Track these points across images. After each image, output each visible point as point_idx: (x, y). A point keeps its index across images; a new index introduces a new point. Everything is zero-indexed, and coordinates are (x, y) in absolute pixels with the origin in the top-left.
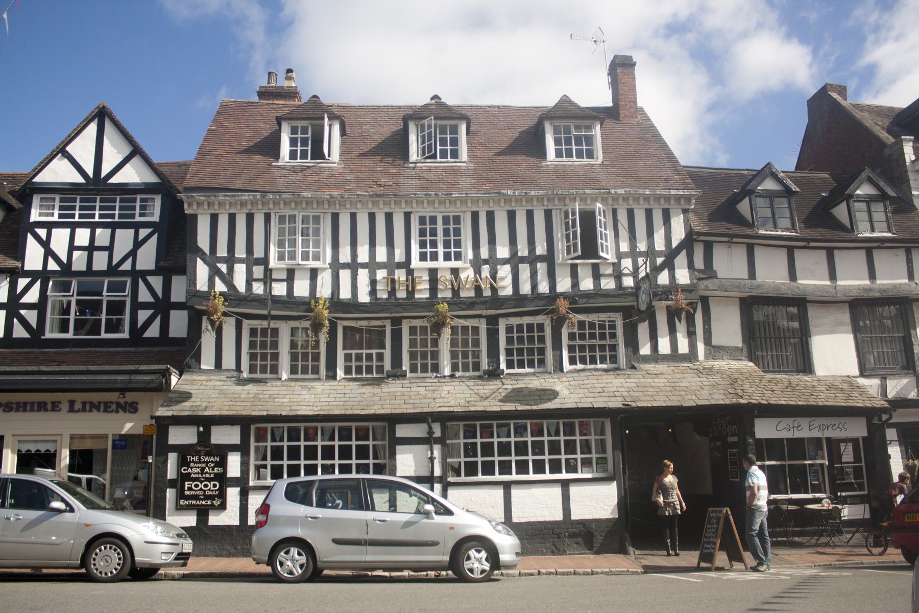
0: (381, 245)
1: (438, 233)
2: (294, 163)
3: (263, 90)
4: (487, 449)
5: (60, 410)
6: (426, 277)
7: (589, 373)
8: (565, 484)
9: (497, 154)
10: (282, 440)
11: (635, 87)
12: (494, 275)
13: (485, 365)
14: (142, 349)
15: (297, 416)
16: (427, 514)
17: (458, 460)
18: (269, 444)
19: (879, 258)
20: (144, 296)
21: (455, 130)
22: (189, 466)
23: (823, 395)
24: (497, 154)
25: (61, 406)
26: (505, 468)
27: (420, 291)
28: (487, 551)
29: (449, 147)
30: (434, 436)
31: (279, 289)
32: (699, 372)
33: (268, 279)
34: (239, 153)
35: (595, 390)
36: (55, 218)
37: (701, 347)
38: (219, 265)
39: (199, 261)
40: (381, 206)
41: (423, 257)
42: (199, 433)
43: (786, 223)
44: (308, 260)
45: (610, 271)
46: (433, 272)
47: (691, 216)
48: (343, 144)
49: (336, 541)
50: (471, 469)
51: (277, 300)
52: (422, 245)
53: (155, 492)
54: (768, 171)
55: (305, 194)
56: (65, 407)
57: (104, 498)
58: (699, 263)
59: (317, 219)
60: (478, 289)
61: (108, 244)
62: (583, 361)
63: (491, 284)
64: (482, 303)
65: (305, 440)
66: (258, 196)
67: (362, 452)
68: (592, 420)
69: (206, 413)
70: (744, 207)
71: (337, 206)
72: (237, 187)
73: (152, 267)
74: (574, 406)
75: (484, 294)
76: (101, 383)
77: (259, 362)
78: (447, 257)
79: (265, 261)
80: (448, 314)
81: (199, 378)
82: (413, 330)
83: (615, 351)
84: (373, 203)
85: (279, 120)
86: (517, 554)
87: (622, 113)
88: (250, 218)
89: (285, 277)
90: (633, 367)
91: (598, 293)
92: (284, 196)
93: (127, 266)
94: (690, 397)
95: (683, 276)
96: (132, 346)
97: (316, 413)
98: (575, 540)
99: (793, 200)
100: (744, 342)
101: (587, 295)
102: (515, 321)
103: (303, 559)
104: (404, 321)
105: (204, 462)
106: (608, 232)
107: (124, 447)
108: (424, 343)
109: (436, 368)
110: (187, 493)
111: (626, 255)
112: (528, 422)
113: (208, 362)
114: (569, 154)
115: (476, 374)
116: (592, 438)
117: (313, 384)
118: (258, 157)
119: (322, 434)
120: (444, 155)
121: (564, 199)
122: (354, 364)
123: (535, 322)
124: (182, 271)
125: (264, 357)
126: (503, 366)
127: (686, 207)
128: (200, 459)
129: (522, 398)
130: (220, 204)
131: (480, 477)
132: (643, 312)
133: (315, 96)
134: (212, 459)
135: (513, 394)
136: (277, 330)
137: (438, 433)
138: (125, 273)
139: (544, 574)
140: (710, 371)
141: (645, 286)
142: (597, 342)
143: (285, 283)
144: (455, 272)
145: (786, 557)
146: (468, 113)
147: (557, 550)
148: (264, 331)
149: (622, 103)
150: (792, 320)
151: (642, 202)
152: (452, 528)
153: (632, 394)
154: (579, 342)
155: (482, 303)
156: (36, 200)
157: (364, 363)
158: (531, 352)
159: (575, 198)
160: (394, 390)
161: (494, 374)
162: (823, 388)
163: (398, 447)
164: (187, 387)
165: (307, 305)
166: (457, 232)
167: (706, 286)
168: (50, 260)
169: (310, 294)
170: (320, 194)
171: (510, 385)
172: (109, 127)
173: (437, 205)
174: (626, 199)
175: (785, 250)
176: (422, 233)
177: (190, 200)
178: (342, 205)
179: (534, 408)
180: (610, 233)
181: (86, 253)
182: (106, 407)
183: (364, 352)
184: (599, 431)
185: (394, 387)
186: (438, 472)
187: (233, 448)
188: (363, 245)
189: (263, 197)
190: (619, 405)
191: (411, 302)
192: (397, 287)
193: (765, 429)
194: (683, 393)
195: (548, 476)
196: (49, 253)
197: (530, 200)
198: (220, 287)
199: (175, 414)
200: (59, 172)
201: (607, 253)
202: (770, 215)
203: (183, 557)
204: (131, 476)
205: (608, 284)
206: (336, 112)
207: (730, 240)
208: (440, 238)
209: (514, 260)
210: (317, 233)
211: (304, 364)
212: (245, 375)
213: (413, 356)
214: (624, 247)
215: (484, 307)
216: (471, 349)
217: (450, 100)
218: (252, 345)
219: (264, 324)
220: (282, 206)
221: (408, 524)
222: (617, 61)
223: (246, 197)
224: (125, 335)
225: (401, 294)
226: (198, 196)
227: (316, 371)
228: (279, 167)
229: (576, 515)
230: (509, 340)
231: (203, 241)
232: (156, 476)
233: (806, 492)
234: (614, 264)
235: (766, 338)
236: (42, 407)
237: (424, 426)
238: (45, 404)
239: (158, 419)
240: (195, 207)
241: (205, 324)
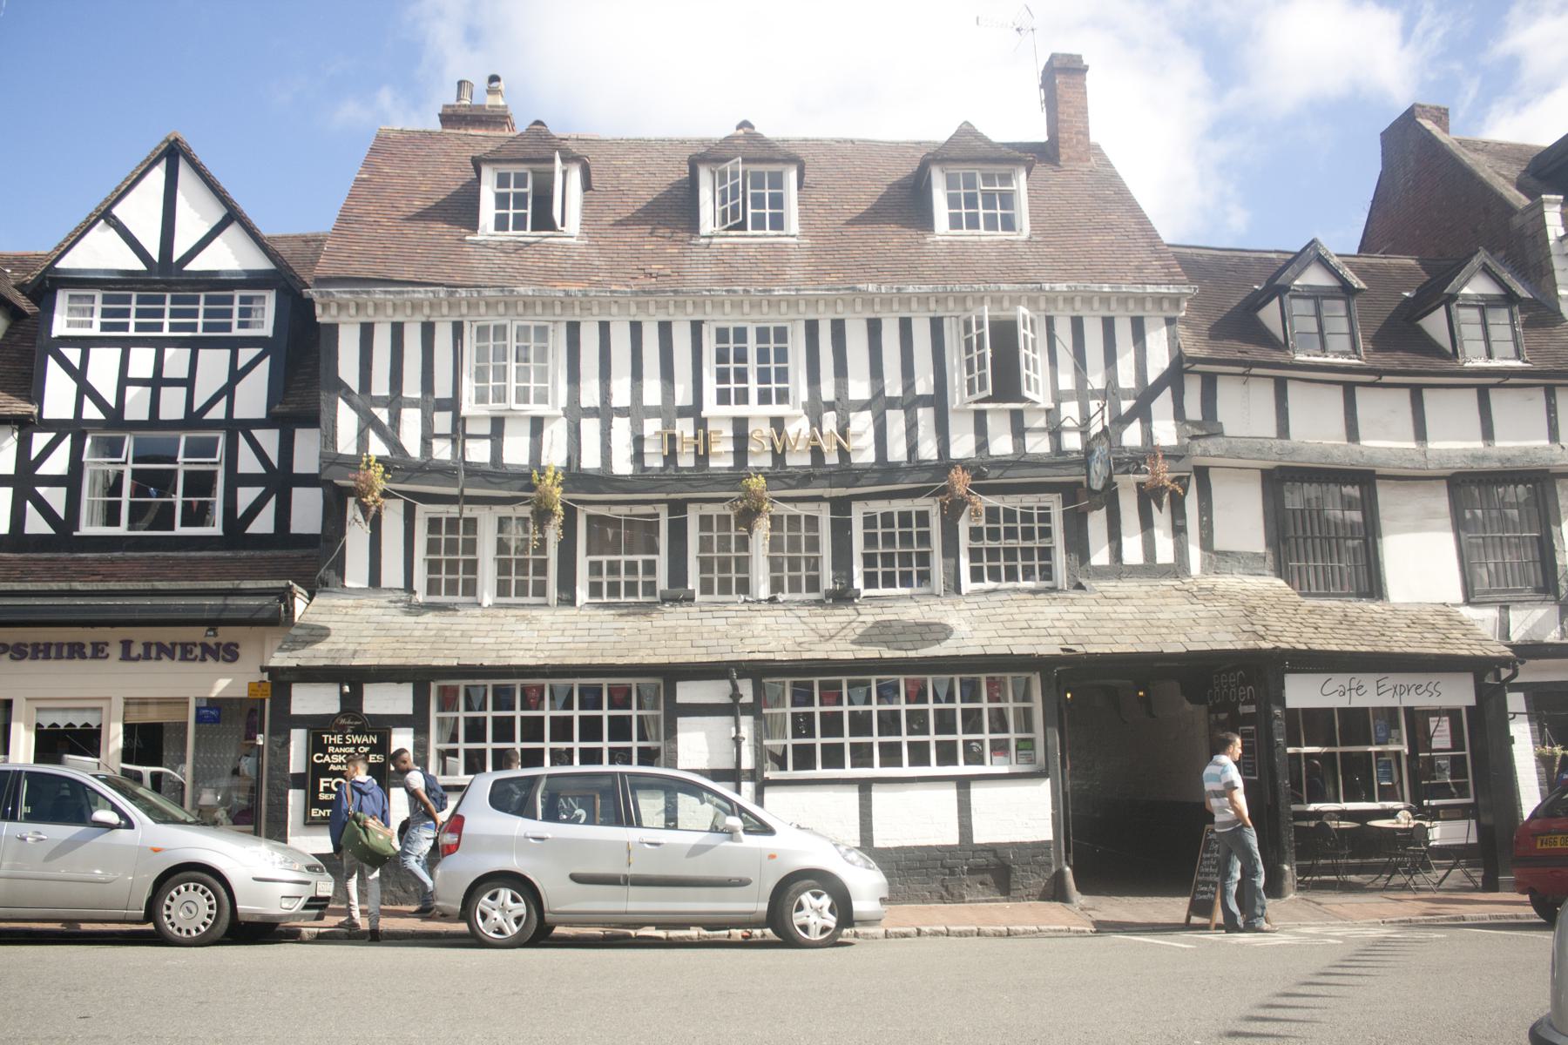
1: (747, 358)
2: (503, 236)
3: (449, 111)
4: (832, 724)
5: (107, 657)
6: (728, 432)
7: (1003, 597)
8: (963, 783)
9: (851, 223)
10: (483, 707)
11: (1086, 108)
12: (843, 431)
13: (827, 581)
14: (244, 554)
15: (509, 667)
16: (730, 833)
17: (782, 742)
18: (462, 714)
19: (1500, 402)
20: (248, 463)
21: (777, 180)
22: (325, 752)
23: (1401, 636)
24: (851, 223)
25: (108, 650)
26: (862, 756)
27: (718, 455)
28: (831, 894)
30: (742, 701)
31: (479, 452)
32: (1191, 596)
34: (409, 219)
35: (1013, 625)
36: (95, 331)
37: (1195, 553)
38: (376, 411)
39: (341, 404)
40: (652, 309)
41: (723, 398)
42: (343, 696)
43: (1343, 343)
44: (527, 401)
45: (1041, 422)
46: (740, 424)
47: (1181, 330)
48: (586, 204)
49: (576, 878)
50: (804, 758)
51: (474, 471)
52: (722, 376)
53: (269, 794)
54: (1312, 254)
55: (522, 290)
56: (115, 651)
57: (182, 805)
58: (1193, 410)
59: (542, 332)
60: (817, 452)
61: (185, 375)
62: (994, 575)
63: (838, 443)
64: (823, 476)
65: (523, 708)
67: (620, 729)
68: (1009, 676)
69: (356, 662)
70: (1270, 315)
71: (577, 311)
72: (406, 277)
73: (260, 413)
74: (979, 651)
75: (827, 462)
76: (176, 610)
77: (443, 576)
78: (764, 398)
79: (453, 404)
80: (766, 495)
81: (342, 602)
82: (705, 522)
83: (1049, 558)
84: (638, 304)
85: (477, 163)
86: (882, 900)
87: (1064, 152)
88: (428, 330)
89: (487, 431)
90: (1079, 587)
91: (1021, 461)
92: (486, 292)
93: (218, 412)
94: (1175, 638)
95: (1166, 432)
96: (227, 549)
97: (541, 662)
98: (980, 877)
99: (1354, 303)
100: (1268, 544)
101: (1002, 464)
102: (879, 507)
103: (520, 908)
104: (690, 507)
105: (351, 745)
106: (1038, 357)
107: (216, 720)
108: (724, 544)
109: (744, 586)
110: (323, 797)
111: (1068, 396)
112: (902, 679)
114: (973, 223)
115: (814, 596)
116: (1010, 706)
117: (535, 613)
118: (441, 227)
119: (552, 698)
120: (759, 223)
121: (965, 298)
122: (605, 579)
123: (1002, 505)
124: (312, 421)
125: (452, 567)
126: (858, 583)
127: (1171, 314)
128: (344, 740)
129: (892, 638)
130: (376, 306)
131: (820, 772)
132: (1096, 492)
133: (538, 123)
134: (365, 739)
135: (876, 631)
136: (474, 521)
137: (747, 697)
138: (215, 425)
139: (927, 934)
140: (1210, 594)
141: (1101, 449)
142: (1019, 543)
143: (488, 442)
144: (778, 423)
145: (1336, 908)
146: (800, 153)
147: (949, 895)
148: (452, 524)
149: (1063, 136)
150: (1350, 509)
151: (1096, 305)
152: (772, 857)
153: (1077, 631)
154: (987, 543)
155: (823, 476)
156: (62, 298)
157: (623, 578)
158: (906, 559)
159: (982, 298)
160: (673, 623)
161: (843, 596)
162: (1401, 623)
163: (680, 720)
164: (322, 618)
166: (782, 355)
167: (1205, 450)
168: (87, 402)
171: (870, 616)
172: (185, 174)
173: (746, 308)
174: (1069, 300)
175: (1340, 389)
176: (722, 357)
177: (325, 300)
178: (586, 308)
179: (912, 654)
180: (1042, 358)
181: (148, 390)
182: (185, 652)
183: (623, 558)
184: (1020, 695)
185: (673, 618)
186: (747, 763)
187: (401, 721)
189: (451, 294)
190: (1056, 651)
191: (702, 475)
192: (678, 448)
193: (1302, 692)
194: (1164, 630)
195: (933, 769)
196: (85, 389)
197: (906, 301)
198: (377, 447)
199: (302, 663)
200: (101, 252)
201: (1037, 392)
202: (1316, 329)
203: (317, 904)
204: (229, 767)
205: (1038, 445)
207: (1247, 370)
208: (752, 365)
209: (879, 404)
210: (542, 355)
211: (520, 578)
212: (421, 597)
213: (705, 565)
214: (1066, 382)
215: (826, 482)
216: (804, 554)
217: (769, 129)
218: (432, 547)
219: (453, 510)
220: (483, 309)
221: (697, 850)
222: (1056, 64)
223: (420, 294)
224: (216, 530)
225: (686, 461)
227: (541, 590)
228: (477, 243)
229: (980, 837)
230: (870, 540)
231: (348, 370)
232: (270, 769)
233: (1371, 799)
234: (1048, 411)
235: (1305, 539)
236: (75, 651)
237: (725, 685)
238: (82, 646)
239: (273, 672)
240: (334, 311)
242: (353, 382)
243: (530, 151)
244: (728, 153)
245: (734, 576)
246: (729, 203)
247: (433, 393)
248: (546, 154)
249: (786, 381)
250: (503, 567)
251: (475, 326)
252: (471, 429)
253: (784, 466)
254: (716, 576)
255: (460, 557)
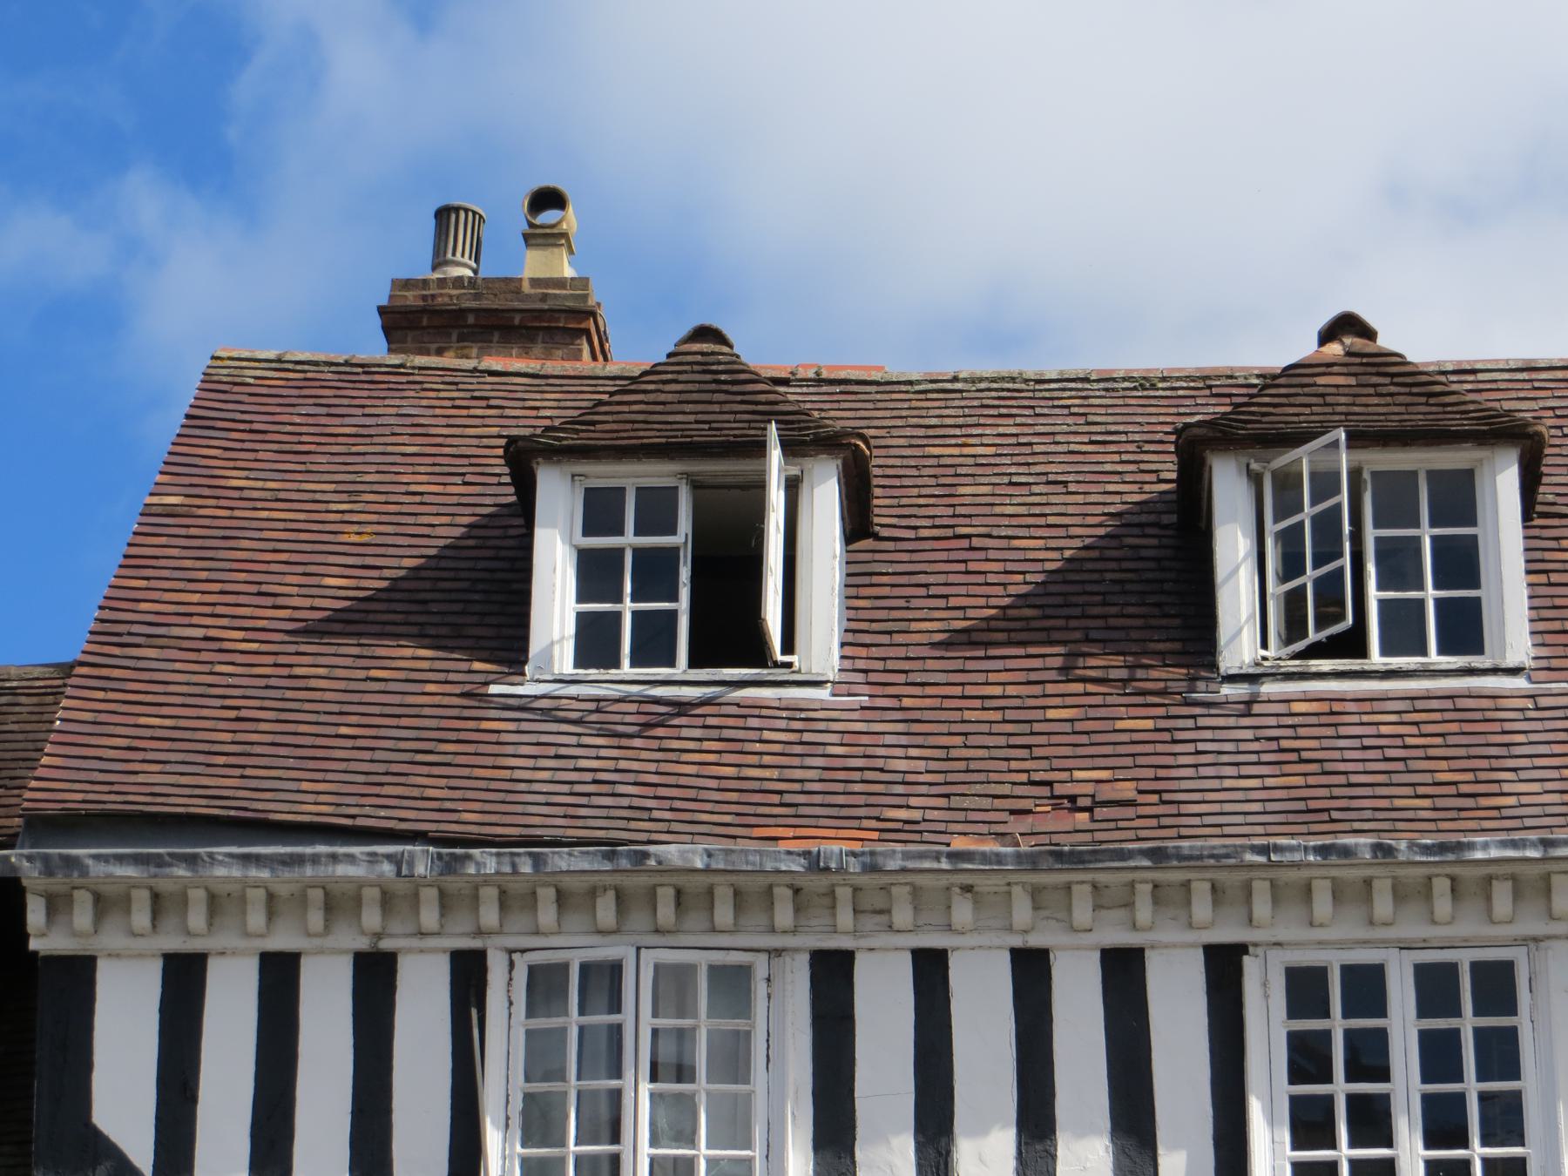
0: (1083, 1132)
2: (601, 684)
3: (411, 298)
21: (1458, 499)
29: (1430, 594)
34: (312, 631)
40: (1082, 912)
48: (857, 580)
55: (672, 852)
59: (733, 985)
66: (422, 860)
71: (845, 918)
72: (308, 812)
84: (1036, 893)
85: (522, 461)
88: (375, 979)
92: (561, 860)
118: (410, 655)
120: (1403, 630)
130: (214, 904)
133: (705, 333)
146: (1525, 410)
170: (750, 853)
173: (1383, 905)
176: (1307, 1059)
177: (58, 883)
178: (873, 910)
188: (981, 1130)
189: (451, 866)
206: (839, 418)
208: (1406, 1087)
210: (733, 1060)
217: (1419, 335)
220: (547, 914)
223: (355, 865)
226: (104, 863)
228: (524, 706)
240: (83, 916)
243: (684, 421)
244: (1294, 415)
246: (1311, 574)
248: (734, 428)
251: (522, 963)
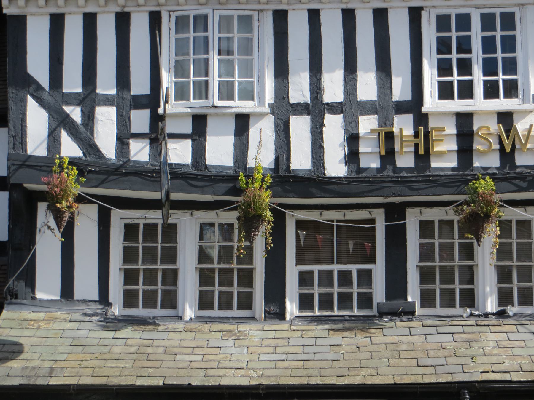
0: (367, 71)
6: (451, 130)
27: (441, 154)
31: (179, 153)
33: (156, 137)
38: (68, 109)
39: (31, 102)
41: (445, 91)
44: (230, 97)
46: (464, 120)
51: (178, 174)
52: (444, 68)
59: (246, 22)
69: (53, 381)
78: (491, 91)
79: (152, 100)
80: (496, 198)
81: (33, 316)
82: (426, 228)
97: (254, 382)
104: (410, 212)
108: (447, 251)
109: (469, 299)
113: (47, 287)
117: (242, 327)
122: (316, 291)
125: (150, 277)
136: (174, 227)
143: (189, 142)
144: (506, 118)
148: (150, 230)
157: (336, 290)
160: (395, 339)
164: (13, 332)
165: (232, 182)
169: (235, 162)
176: (443, 46)
183: (336, 268)
185: (393, 334)
188: (332, 70)
192: (397, 147)
198: (70, 148)
208: (477, 56)
210: (247, 48)
211: (226, 291)
212: (117, 310)
213: (426, 276)
218: (129, 255)
219: (154, 217)
225: (405, 161)
227: (246, 302)
231: (37, 65)
241: (43, 215)
242: (44, 80)
245: (457, 287)
247: (129, 89)
249: (515, 73)
250: (205, 278)
251: (173, 16)
252: (170, 127)
253: (514, 166)
254: (438, 287)
255: (159, 266)
